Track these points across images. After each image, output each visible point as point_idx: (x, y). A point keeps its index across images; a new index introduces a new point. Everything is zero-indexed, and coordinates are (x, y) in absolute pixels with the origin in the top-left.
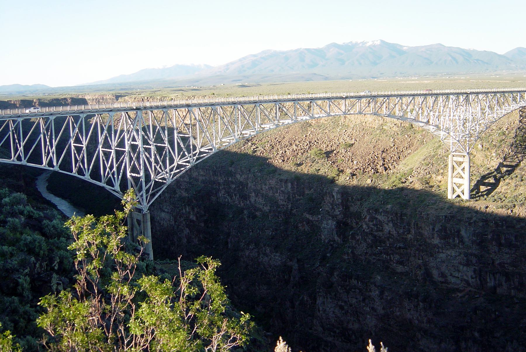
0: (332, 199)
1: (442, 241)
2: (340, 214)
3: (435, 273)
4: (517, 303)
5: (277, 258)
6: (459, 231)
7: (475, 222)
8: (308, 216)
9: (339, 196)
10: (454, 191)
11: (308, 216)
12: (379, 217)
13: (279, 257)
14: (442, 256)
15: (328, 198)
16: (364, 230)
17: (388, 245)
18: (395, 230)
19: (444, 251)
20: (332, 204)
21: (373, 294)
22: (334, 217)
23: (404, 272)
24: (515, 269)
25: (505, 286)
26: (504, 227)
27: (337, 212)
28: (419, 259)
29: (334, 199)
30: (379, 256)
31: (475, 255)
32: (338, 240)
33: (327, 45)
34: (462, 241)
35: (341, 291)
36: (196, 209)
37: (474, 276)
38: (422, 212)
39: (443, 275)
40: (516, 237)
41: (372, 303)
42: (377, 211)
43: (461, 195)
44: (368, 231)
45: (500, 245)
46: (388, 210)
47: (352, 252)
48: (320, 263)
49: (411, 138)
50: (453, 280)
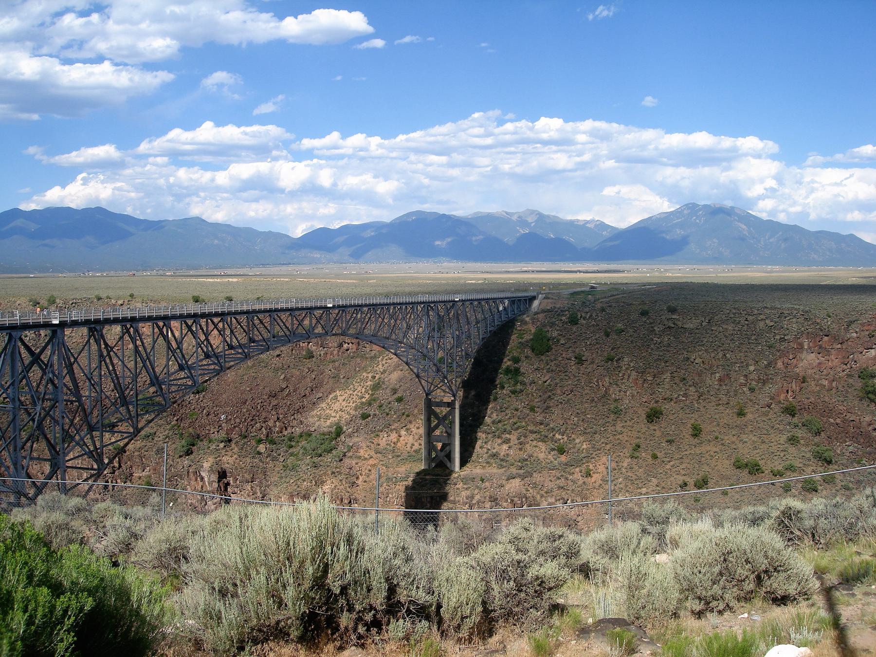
0: (201, 484)
9: (215, 477)
15: (193, 483)
29: (204, 483)
33: (541, 217)
38: (388, 494)
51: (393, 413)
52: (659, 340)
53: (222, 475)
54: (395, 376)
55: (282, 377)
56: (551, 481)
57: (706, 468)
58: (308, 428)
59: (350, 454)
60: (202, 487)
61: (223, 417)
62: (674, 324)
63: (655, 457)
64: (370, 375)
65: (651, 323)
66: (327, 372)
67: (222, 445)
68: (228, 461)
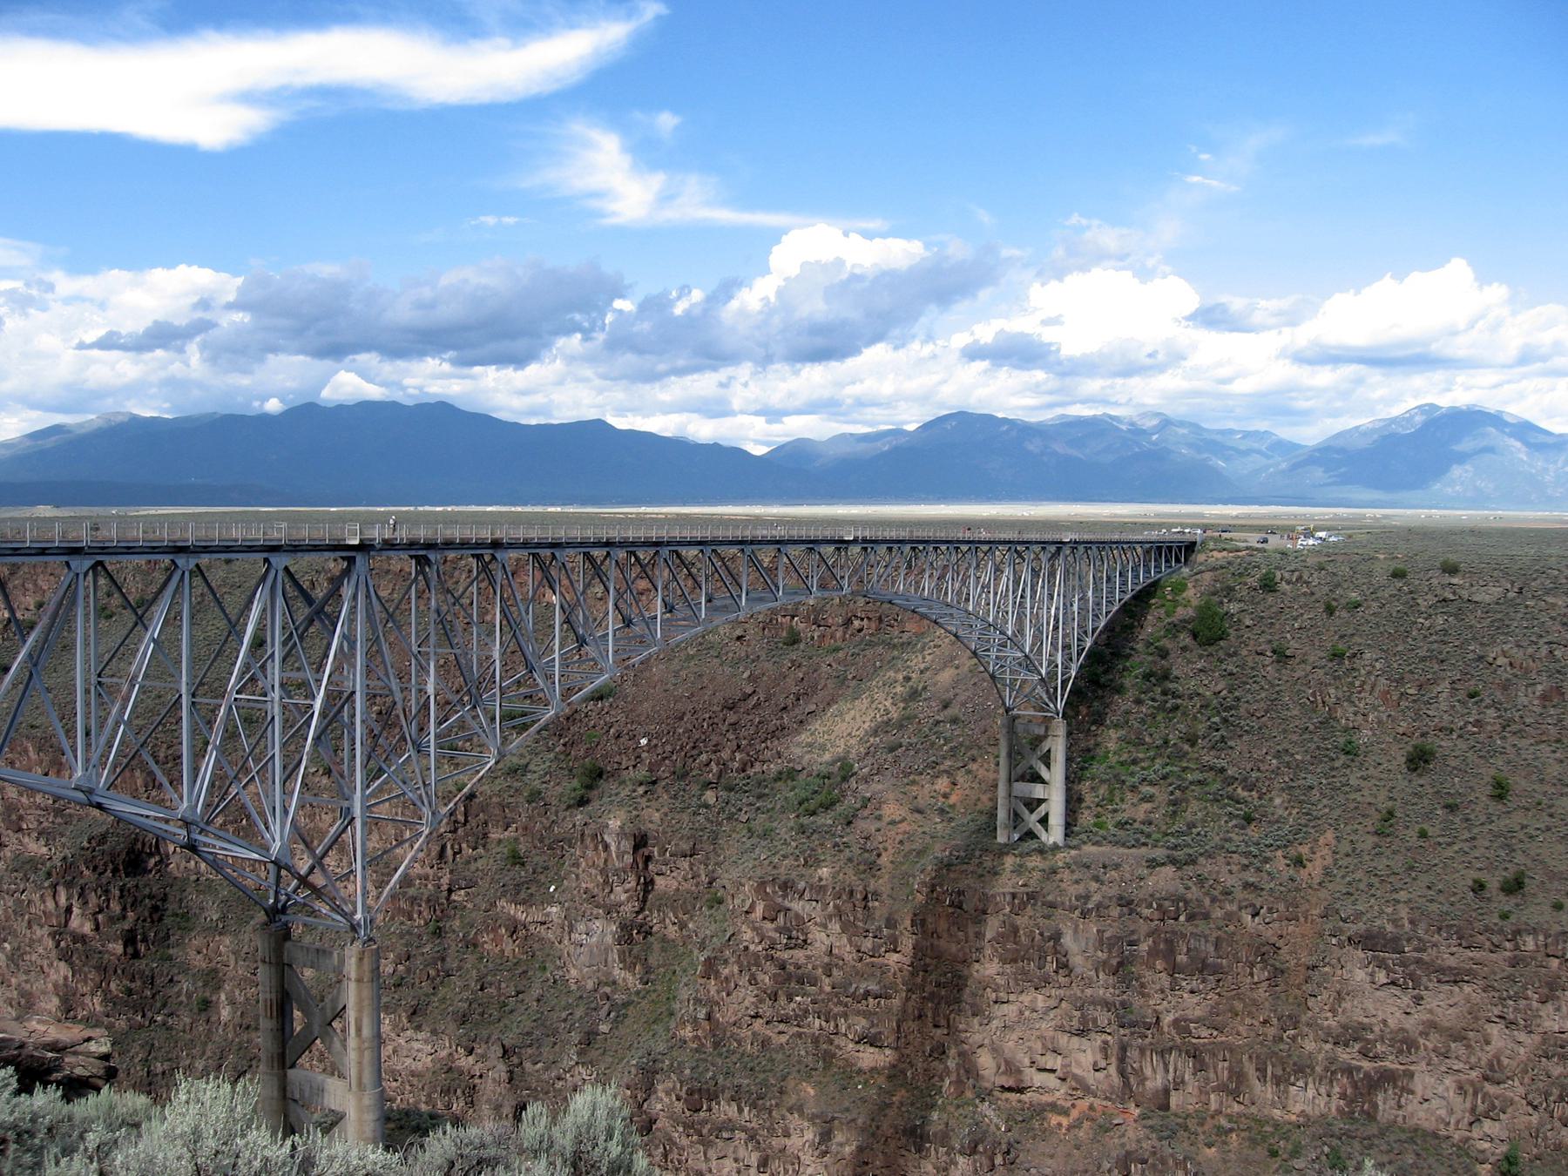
1: (1008, 968)
2: (628, 900)
3: (985, 1061)
4: (1231, 1130)
5: (416, 1045)
6: (1057, 937)
7: (1099, 906)
8: (513, 910)
9: (627, 845)
10: (1016, 818)
11: (513, 910)
12: (797, 906)
13: (426, 1042)
14: (1010, 1010)
15: (589, 853)
16: (746, 948)
17: (828, 989)
18: (850, 941)
19: (1012, 998)
20: (603, 872)
21: (794, 1142)
22: (610, 910)
23: (884, 1068)
24: (1215, 1033)
25: (1192, 1085)
26: (1182, 918)
27: (620, 894)
28: (936, 1026)
29: (610, 855)
30: (798, 1026)
31: (1108, 1005)
32: (624, 980)
34: (1064, 966)
35: (685, 1141)
36: (93, 900)
37: (1102, 1064)
39: (1011, 1068)
40: (1217, 946)
41: (794, 1170)
42: (787, 886)
43: (1038, 829)
44: (760, 948)
45: (1173, 969)
46: (823, 883)
47: (709, 1017)
48: (579, 1054)
49: (804, 669)
50: (1039, 1079)
51: (942, 742)
52: (1427, 623)
53: (640, 842)
54: (946, 676)
55: (745, 675)
56: (1230, 872)
57: (1519, 858)
58: (791, 765)
59: (866, 813)
60: (606, 861)
61: (644, 741)
62: (1454, 593)
63: (1423, 834)
64: (900, 677)
65: (1411, 592)
66: (824, 668)
67: (641, 790)
68: (653, 817)
